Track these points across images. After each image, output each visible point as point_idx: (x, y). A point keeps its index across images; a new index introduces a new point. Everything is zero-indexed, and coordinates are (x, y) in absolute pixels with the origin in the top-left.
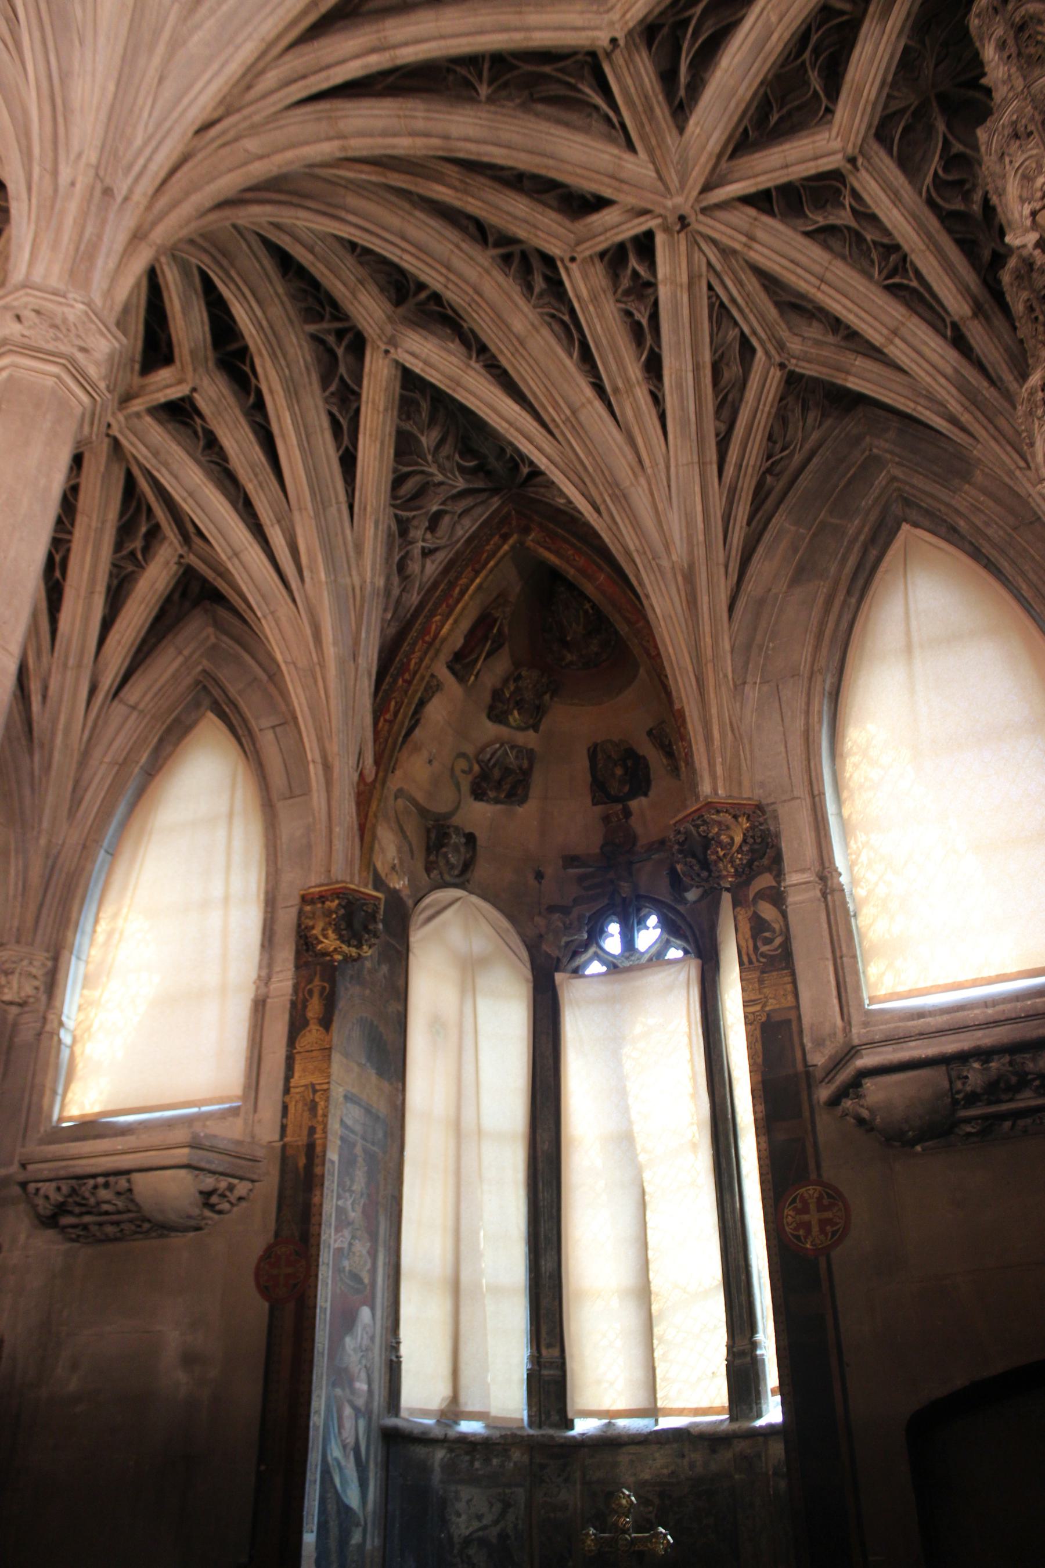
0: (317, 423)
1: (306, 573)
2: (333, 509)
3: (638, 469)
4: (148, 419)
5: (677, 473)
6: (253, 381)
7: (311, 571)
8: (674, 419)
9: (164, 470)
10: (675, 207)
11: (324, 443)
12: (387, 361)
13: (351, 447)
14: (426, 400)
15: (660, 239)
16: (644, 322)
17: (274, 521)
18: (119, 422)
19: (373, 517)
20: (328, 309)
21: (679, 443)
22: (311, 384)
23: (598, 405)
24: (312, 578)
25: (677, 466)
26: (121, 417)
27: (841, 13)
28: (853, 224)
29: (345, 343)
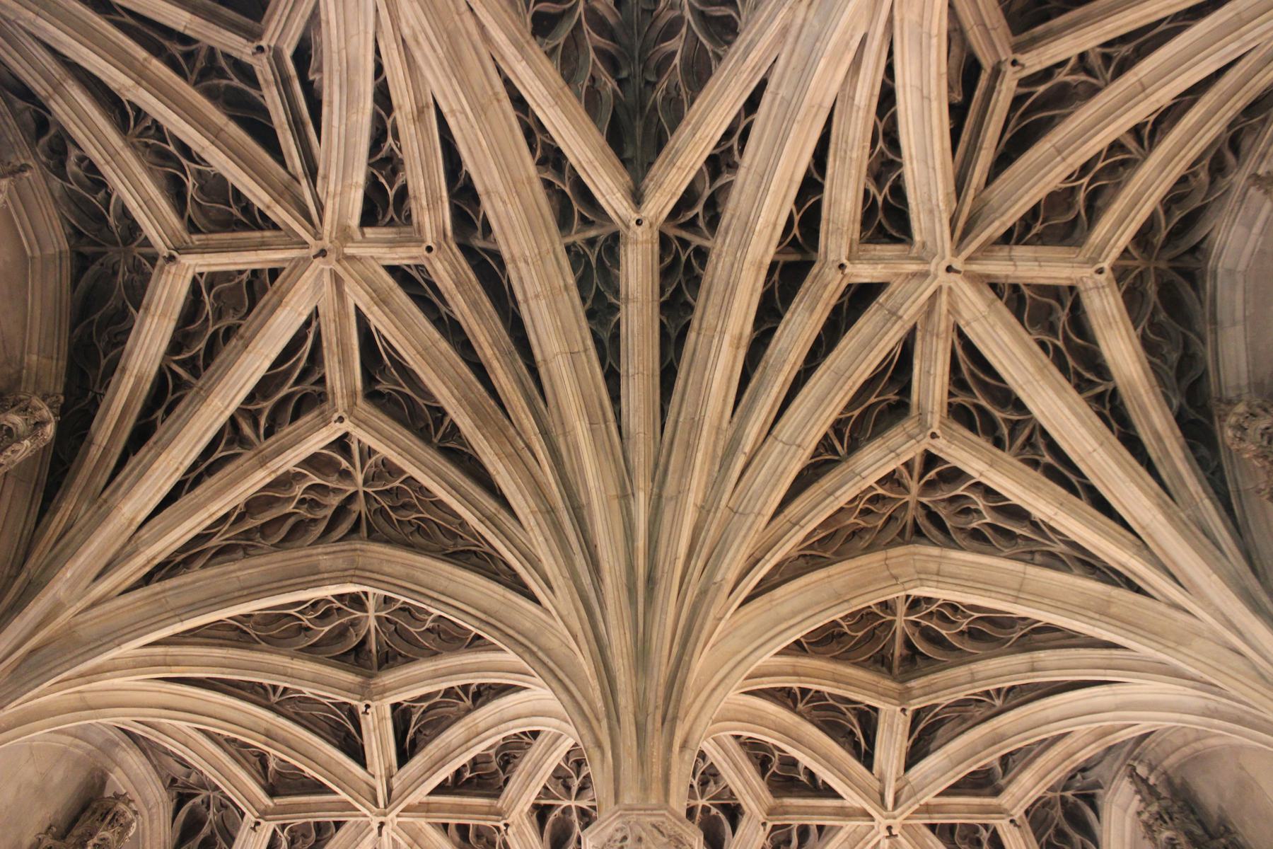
0: (750, 177)
1: (855, 44)
2: (782, 92)
3: (410, 42)
4: (917, 238)
5: (366, 26)
6: (797, 218)
7: (848, 43)
8: (365, 71)
9: (934, 201)
10: (328, 263)
11: (755, 155)
12: (644, 214)
13: (743, 115)
14: (655, 101)
15: (355, 221)
16: (390, 140)
17: (855, 109)
18: (937, 265)
19: (743, 68)
20: (684, 258)
21: (361, 51)
22: (733, 216)
23: (445, 109)
24: (852, 37)
25: (366, 33)
26: (932, 268)
27: (176, 362)
28: (185, 162)
29: (691, 214)
